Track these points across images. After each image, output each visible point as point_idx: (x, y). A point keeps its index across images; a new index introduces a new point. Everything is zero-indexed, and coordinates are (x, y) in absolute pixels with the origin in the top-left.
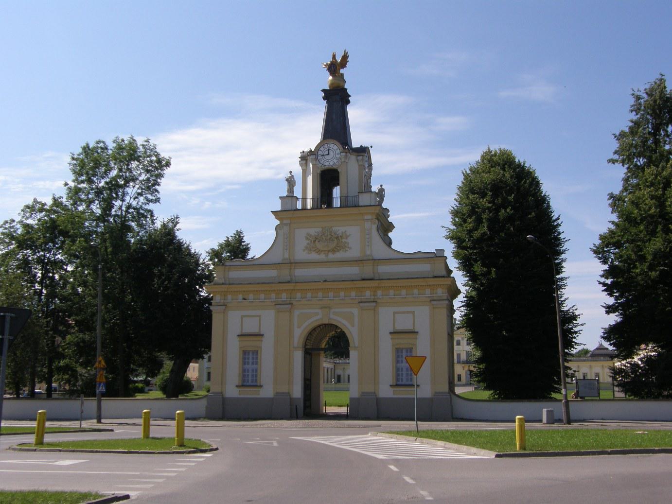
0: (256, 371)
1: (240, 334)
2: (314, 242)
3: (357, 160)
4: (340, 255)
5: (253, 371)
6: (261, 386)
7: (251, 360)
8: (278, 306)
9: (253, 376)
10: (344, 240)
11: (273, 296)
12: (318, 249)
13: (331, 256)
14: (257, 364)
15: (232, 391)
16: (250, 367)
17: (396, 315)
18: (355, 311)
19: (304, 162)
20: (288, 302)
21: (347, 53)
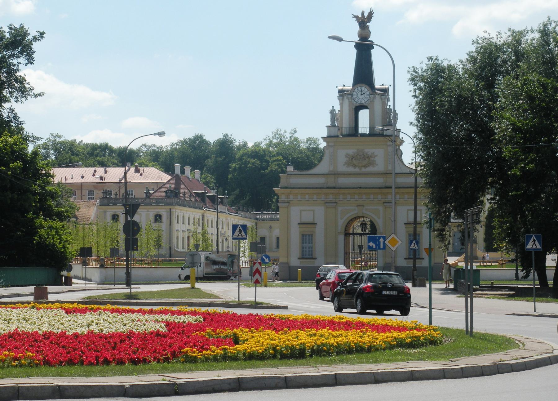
0: (312, 248)
1: (299, 223)
2: (352, 160)
3: (381, 98)
4: (370, 169)
5: (309, 248)
6: (316, 258)
7: (307, 241)
8: (327, 204)
9: (309, 251)
10: (372, 159)
11: (323, 197)
12: (354, 164)
13: (364, 170)
14: (312, 243)
15: (295, 261)
16: (307, 245)
17: (409, 212)
18: (381, 208)
19: (341, 97)
20: (334, 201)
21: (373, 13)
